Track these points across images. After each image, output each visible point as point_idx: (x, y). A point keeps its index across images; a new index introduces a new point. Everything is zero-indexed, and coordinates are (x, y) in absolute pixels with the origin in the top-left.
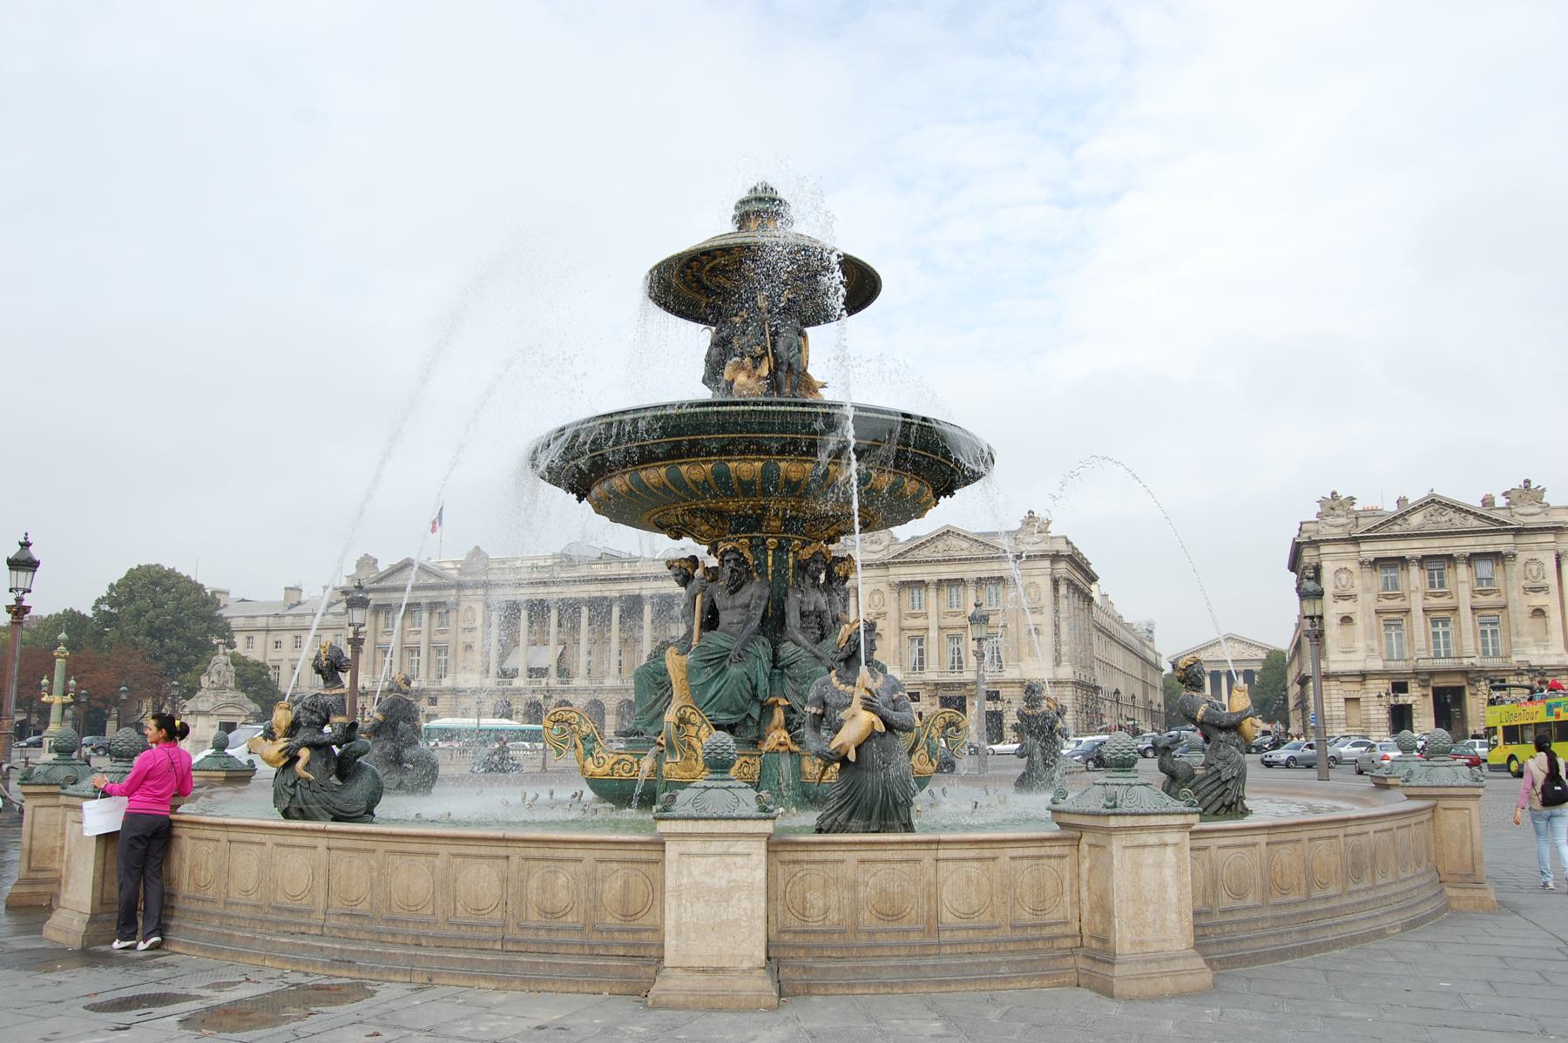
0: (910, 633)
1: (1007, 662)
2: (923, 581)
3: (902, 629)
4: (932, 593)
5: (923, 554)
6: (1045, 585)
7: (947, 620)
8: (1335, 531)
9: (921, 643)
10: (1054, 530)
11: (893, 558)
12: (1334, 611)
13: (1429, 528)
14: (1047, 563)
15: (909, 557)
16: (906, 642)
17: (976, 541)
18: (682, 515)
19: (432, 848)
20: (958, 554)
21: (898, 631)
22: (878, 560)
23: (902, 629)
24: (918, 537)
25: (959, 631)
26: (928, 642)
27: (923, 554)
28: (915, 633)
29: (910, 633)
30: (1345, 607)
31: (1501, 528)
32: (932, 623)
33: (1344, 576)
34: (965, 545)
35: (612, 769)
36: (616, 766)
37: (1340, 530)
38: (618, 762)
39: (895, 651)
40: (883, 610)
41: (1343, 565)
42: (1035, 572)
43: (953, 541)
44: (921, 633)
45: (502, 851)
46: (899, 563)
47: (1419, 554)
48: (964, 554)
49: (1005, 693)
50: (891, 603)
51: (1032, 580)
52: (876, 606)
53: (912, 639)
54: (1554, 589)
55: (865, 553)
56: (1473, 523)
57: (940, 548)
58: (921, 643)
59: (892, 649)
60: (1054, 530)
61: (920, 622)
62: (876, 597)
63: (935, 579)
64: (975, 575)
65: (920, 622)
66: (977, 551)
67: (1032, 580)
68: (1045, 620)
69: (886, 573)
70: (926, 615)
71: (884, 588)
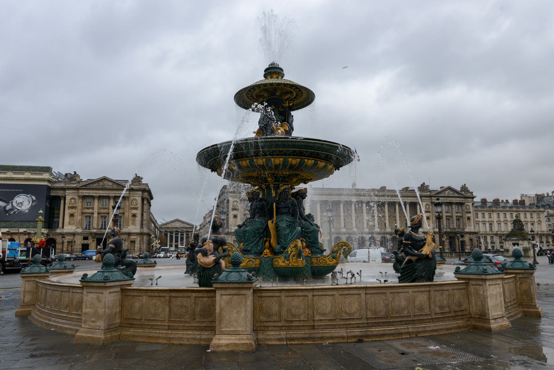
0: (85, 215)
1: (123, 226)
2: (93, 196)
3: (83, 213)
4: (96, 201)
6: (139, 200)
7: (101, 211)
9: (90, 218)
10: (144, 181)
11: (82, 186)
12: (232, 213)
14: (140, 193)
16: (84, 218)
17: (115, 183)
18: (268, 175)
19: (406, 290)
20: (108, 187)
21: (81, 214)
22: (75, 187)
23: (83, 213)
24: (93, 180)
25: (106, 215)
26: (93, 218)
28: (88, 215)
29: (85, 215)
30: (235, 212)
32: (96, 211)
34: (110, 184)
35: (247, 264)
36: (248, 263)
38: (248, 261)
39: (79, 221)
40: (75, 205)
41: (427, 203)
42: (136, 195)
43: (107, 182)
44: (90, 215)
45: (428, 289)
46: (84, 188)
48: (111, 187)
50: (79, 204)
51: (135, 198)
52: (72, 204)
53: (86, 217)
58: (90, 218)
59: (78, 220)
60: (144, 181)
61: (90, 211)
62: (73, 201)
63: (98, 195)
64: (114, 195)
65: (90, 211)
66: (115, 187)
67: (135, 198)
68: (138, 212)
69: (78, 192)
70: (93, 208)
71: (76, 197)
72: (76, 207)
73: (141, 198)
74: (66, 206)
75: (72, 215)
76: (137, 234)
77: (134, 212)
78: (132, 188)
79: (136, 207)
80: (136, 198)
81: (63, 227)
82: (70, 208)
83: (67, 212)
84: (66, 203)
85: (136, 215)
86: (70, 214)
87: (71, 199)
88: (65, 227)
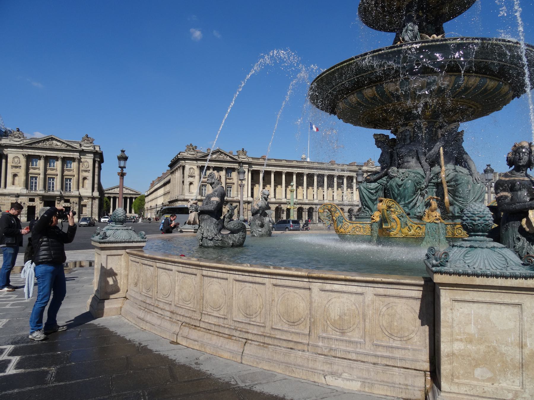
5: (40, 145)
6: (91, 162)
8: (190, 156)
12: (188, 180)
13: (217, 159)
15: (33, 146)
27: (40, 145)
30: (191, 179)
31: (235, 161)
33: (192, 170)
34: (59, 144)
37: (192, 156)
40: (19, 165)
47: (213, 166)
49: (72, 200)
51: (86, 160)
52: (16, 163)
54: (247, 180)
55: (11, 141)
56: (228, 159)
57: (47, 144)
62: (16, 160)
63: (45, 155)
66: (63, 147)
68: (89, 175)
72: (20, 167)
73: (92, 160)
74: (8, 165)
75: (15, 175)
76: (89, 198)
77: (85, 174)
78: (83, 150)
79: (87, 169)
80: (87, 160)
81: (5, 186)
82: (13, 167)
83: (10, 171)
84: (8, 162)
85: (87, 177)
86: (13, 174)
87: (14, 158)
88: (7, 187)
